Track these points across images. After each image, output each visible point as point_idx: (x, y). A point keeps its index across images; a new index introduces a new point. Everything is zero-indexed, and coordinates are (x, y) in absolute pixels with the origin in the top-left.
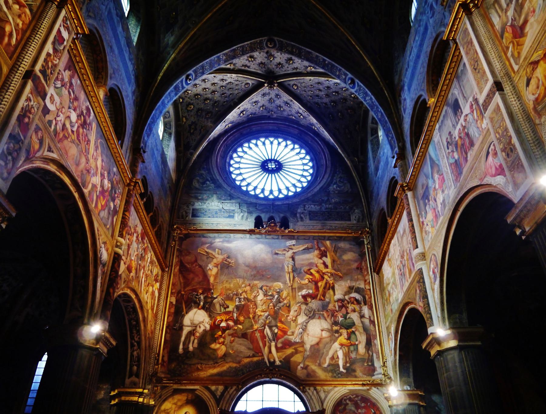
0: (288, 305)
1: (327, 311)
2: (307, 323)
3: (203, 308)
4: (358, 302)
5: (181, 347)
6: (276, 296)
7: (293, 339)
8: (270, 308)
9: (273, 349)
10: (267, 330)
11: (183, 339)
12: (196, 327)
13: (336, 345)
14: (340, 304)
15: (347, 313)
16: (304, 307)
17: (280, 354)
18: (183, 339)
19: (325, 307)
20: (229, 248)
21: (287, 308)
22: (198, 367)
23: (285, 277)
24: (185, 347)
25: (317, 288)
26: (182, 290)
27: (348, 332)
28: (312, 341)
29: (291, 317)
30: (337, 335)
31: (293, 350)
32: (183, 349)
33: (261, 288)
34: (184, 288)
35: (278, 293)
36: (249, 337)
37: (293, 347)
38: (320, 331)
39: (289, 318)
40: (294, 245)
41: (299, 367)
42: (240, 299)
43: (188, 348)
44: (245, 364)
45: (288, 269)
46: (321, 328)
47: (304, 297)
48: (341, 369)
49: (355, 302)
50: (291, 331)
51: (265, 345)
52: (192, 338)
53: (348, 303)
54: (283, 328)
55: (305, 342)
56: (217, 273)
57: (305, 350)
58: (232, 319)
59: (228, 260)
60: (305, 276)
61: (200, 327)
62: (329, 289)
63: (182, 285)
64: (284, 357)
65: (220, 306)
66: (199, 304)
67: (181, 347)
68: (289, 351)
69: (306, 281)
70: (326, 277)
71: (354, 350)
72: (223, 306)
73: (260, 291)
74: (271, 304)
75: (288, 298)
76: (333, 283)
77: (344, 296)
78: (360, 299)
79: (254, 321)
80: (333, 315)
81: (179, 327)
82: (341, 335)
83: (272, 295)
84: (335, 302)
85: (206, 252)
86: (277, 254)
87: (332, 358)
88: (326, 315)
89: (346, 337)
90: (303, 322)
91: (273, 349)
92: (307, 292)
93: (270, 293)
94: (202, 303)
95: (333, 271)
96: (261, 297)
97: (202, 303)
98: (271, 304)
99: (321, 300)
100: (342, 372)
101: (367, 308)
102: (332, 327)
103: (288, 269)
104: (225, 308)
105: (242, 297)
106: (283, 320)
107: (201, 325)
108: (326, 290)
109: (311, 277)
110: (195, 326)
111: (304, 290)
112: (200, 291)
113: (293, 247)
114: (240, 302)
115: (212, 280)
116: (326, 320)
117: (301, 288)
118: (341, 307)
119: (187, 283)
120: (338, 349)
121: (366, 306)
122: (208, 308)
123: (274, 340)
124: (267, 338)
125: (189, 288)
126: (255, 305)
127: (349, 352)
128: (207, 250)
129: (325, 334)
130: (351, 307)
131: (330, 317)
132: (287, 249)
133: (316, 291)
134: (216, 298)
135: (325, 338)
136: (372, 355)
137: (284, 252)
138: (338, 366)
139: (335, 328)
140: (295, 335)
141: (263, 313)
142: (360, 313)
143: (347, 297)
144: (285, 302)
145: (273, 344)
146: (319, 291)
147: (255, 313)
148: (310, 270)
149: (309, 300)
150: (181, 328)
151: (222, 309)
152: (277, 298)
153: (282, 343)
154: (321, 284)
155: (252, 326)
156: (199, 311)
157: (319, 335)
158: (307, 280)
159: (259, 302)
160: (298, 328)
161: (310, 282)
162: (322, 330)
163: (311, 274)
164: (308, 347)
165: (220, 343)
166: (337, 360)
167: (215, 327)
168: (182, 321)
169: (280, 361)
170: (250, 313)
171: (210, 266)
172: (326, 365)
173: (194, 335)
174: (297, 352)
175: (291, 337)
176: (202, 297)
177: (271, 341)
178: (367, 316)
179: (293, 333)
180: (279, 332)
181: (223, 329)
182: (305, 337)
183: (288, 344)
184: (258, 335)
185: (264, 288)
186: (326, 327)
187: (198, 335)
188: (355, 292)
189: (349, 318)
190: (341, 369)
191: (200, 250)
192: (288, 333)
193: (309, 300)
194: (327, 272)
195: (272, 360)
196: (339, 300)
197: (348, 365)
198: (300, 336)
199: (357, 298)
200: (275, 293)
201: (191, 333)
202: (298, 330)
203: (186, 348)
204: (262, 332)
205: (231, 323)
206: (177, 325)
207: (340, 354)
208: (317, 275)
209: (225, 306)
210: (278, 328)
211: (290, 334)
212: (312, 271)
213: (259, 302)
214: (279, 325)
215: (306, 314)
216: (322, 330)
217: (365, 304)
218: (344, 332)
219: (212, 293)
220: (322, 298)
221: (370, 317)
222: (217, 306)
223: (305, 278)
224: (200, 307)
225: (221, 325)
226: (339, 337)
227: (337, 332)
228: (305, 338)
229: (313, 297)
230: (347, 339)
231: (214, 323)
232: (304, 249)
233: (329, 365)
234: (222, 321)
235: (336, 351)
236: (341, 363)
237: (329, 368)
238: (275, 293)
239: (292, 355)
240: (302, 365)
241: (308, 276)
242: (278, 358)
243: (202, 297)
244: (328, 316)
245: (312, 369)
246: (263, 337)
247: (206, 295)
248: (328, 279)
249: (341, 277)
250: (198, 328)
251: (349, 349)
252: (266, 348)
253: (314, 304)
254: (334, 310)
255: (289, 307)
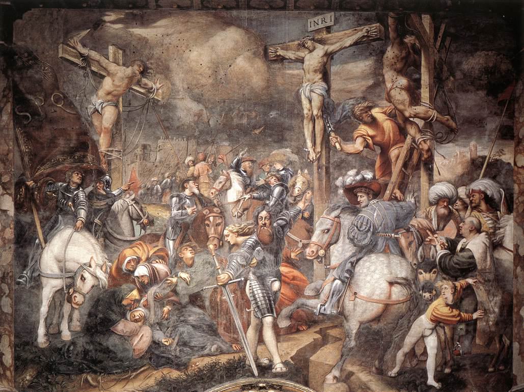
0: (306, 215)
1: (408, 230)
2: (354, 265)
3: (88, 226)
4: (491, 203)
5: (41, 331)
6: (277, 190)
7: (315, 304)
8: (261, 223)
9: (269, 335)
10: (253, 287)
11: (44, 309)
12: (72, 278)
13: (424, 322)
14: (442, 211)
15: (460, 236)
16: (347, 220)
17: (284, 345)
18: (44, 309)
19: (400, 223)
20: (144, 41)
21: (304, 223)
22: (86, 381)
23: (301, 129)
24: (51, 331)
25: (387, 165)
26: (28, 173)
27: (455, 287)
28: (364, 312)
29: (314, 248)
30: (427, 295)
31: (318, 336)
32: (47, 334)
33: (237, 168)
34: (33, 169)
35: (282, 181)
36: (207, 303)
37: (318, 329)
38: (385, 285)
39: (308, 251)
40: (328, 29)
41: (330, 377)
42: (181, 199)
43: (60, 332)
44: (200, 370)
45: (310, 109)
46: (390, 278)
47: (351, 191)
48: (431, 381)
49: (483, 206)
50: (313, 285)
51: (246, 326)
52: (67, 308)
53: (466, 208)
54: (294, 278)
55: (347, 313)
56: (117, 123)
57: (347, 335)
58: (162, 257)
59: (144, 80)
60: (356, 128)
61: (83, 279)
62: (417, 168)
63: (26, 159)
64: (293, 353)
65: (131, 218)
66: (75, 216)
67: (41, 331)
68: (307, 338)
69: (358, 145)
70: (412, 131)
71: (467, 332)
72: (138, 219)
73: (234, 176)
74: (264, 214)
75: (308, 195)
76: (429, 150)
77: (456, 187)
78: (496, 197)
79: (221, 262)
80: (422, 241)
81: (32, 278)
82: (437, 296)
83: (267, 187)
84: (431, 204)
85: (81, 55)
86: (281, 59)
87: (412, 354)
88: (403, 242)
89: (450, 301)
90: (346, 261)
91: (269, 335)
92: (358, 178)
93: (261, 182)
94: (83, 213)
95: (434, 113)
96: (235, 192)
97: (83, 213)
98: (264, 214)
99: (396, 198)
100: (431, 387)
101: (511, 222)
102: (415, 271)
103: (310, 109)
104: (144, 227)
105: (187, 192)
106: (293, 255)
107: (87, 275)
108: (409, 171)
109: (371, 132)
110: (71, 278)
111: (352, 172)
112: (76, 178)
113: (324, 35)
114: (182, 208)
115: (103, 142)
116: (402, 254)
117: (342, 166)
118: (444, 220)
119: (36, 159)
120: (428, 332)
121: (512, 216)
122: (101, 227)
123: (271, 311)
124: (253, 306)
125: (44, 170)
126: (222, 214)
127: (452, 339)
128: (84, 51)
129: (398, 293)
130: (470, 218)
131: (413, 245)
132: (309, 44)
133: (383, 175)
134: (119, 196)
135: (399, 302)
136: (510, 347)
137: (301, 54)
138: (425, 372)
139: (424, 277)
140: (322, 296)
141: (241, 239)
142: (491, 235)
143: (462, 192)
144: (301, 206)
145: (268, 320)
146: (390, 174)
147: (221, 238)
148: (370, 108)
149: (363, 198)
150: (37, 282)
151: (137, 228)
152: (281, 194)
153: (290, 317)
154: (397, 153)
155: (214, 274)
156: (77, 236)
157: (383, 297)
158: (359, 140)
159: (231, 207)
160: (330, 278)
161: (367, 146)
162: (391, 284)
163: (373, 123)
164: (353, 326)
165: (136, 321)
166: (423, 358)
167: (121, 276)
168: (38, 261)
169: (285, 363)
170: (208, 239)
171: (97, 101)
172: (393, 372)
173: (70, 301)
174: (325, 340)
175: (311, 302)
176: (82, 196)
177: (263, 315)
178: (509, 243)
179: (317, 295)
180: (286, 291)
181: (142, 284)
182: (347, 301)
183: (303, 321)
184: (228, 297)
185: (246, 165)
186: (403, 275)
187: (79, 298)
188: (484, 176)
189: (463, 250)
190: (431, 381)
191: (65, 51)
192: (308, 292)
193: (363, 198)
194: (416, 116)
195: (265, 361)
196: (440, 200)
197: (447, 371)
198: (335, 299)
199: (489, 193)
200: (273, 181)
201: (64, 296)
202: (331, 284)
203: (54, 334)
204: (241, 287)
205: (161, 267)
206: (27, 273)
207: (432, 343)
208: (388, 125)
209: (145, 221)
210: (280, 281)
211: (311, 293)
212: (376, 112)
213: (231, 207)
214: (284, 269)
215: (352, 240)
216: (391, 284)
217: (510, 210)
218: (447, 289)
219: (108, 184)
220: (398, 194)
221: (517, 246)
222: (124, 221)
223: (356, 134)
224: (79, 224)
225: (136, 274)
226: (431, 300)
227: (428, 287)
228: (349, 304)
229: (376, 194)
230: (452, 307)
231: (119, 269)
232: (356, 44)
233: (400, 373)
234: (138, 261)
235: (423, 337)
236: (431, 365)
237: (401, 379)
238: (273, 181)
239: (315, 347)
240: (336, 373)
241: (364, 129)
242: (281, 356)
243: (82, 196)
244: (410, 244)
245: (361, 381)
246: (243, 302)
247: (90, 189)
248: (418, 137)
249: (452, 130)
250: (79, 282)
251: (454, 329)
252: (251, 332)
253: (375, 211)
254: (425, 229)
255: (310, 220)
